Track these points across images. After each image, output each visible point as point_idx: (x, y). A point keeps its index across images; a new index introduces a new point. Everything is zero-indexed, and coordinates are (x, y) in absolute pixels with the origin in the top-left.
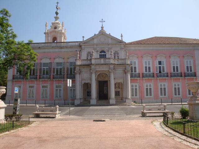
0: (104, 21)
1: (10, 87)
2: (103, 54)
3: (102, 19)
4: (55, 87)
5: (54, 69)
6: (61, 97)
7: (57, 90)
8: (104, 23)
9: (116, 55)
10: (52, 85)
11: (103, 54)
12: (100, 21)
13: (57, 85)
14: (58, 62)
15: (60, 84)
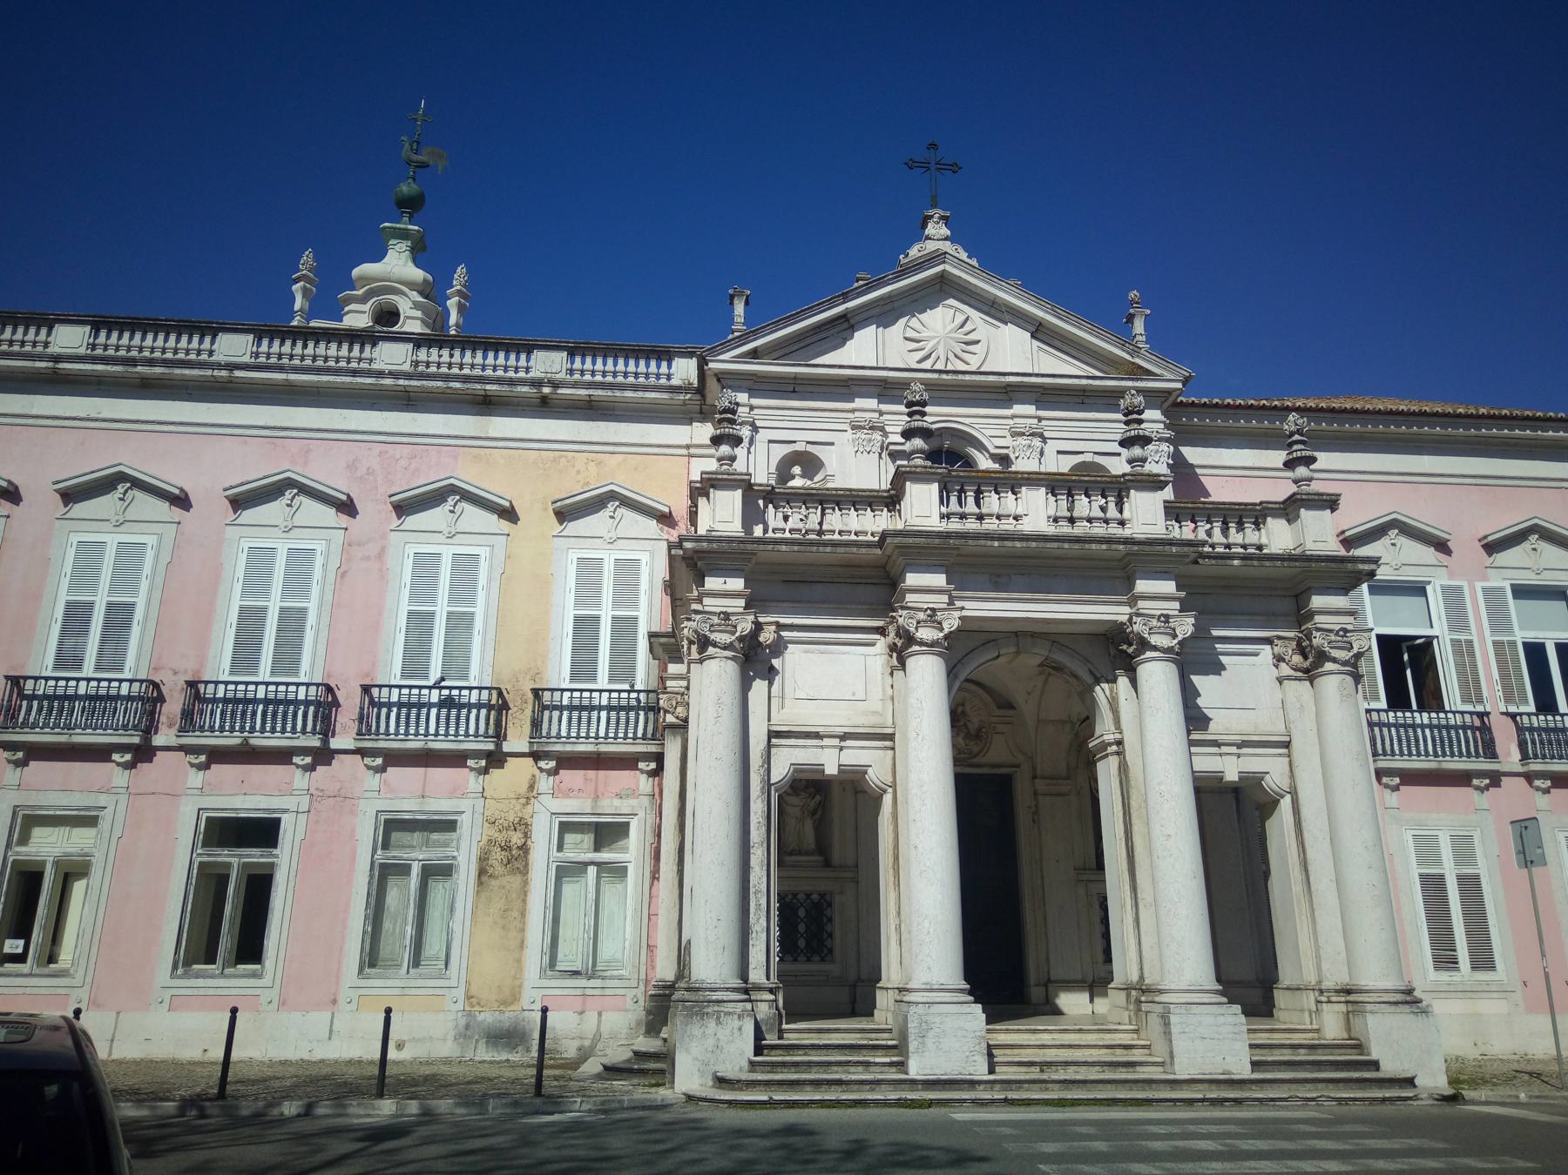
15: (439, 805)
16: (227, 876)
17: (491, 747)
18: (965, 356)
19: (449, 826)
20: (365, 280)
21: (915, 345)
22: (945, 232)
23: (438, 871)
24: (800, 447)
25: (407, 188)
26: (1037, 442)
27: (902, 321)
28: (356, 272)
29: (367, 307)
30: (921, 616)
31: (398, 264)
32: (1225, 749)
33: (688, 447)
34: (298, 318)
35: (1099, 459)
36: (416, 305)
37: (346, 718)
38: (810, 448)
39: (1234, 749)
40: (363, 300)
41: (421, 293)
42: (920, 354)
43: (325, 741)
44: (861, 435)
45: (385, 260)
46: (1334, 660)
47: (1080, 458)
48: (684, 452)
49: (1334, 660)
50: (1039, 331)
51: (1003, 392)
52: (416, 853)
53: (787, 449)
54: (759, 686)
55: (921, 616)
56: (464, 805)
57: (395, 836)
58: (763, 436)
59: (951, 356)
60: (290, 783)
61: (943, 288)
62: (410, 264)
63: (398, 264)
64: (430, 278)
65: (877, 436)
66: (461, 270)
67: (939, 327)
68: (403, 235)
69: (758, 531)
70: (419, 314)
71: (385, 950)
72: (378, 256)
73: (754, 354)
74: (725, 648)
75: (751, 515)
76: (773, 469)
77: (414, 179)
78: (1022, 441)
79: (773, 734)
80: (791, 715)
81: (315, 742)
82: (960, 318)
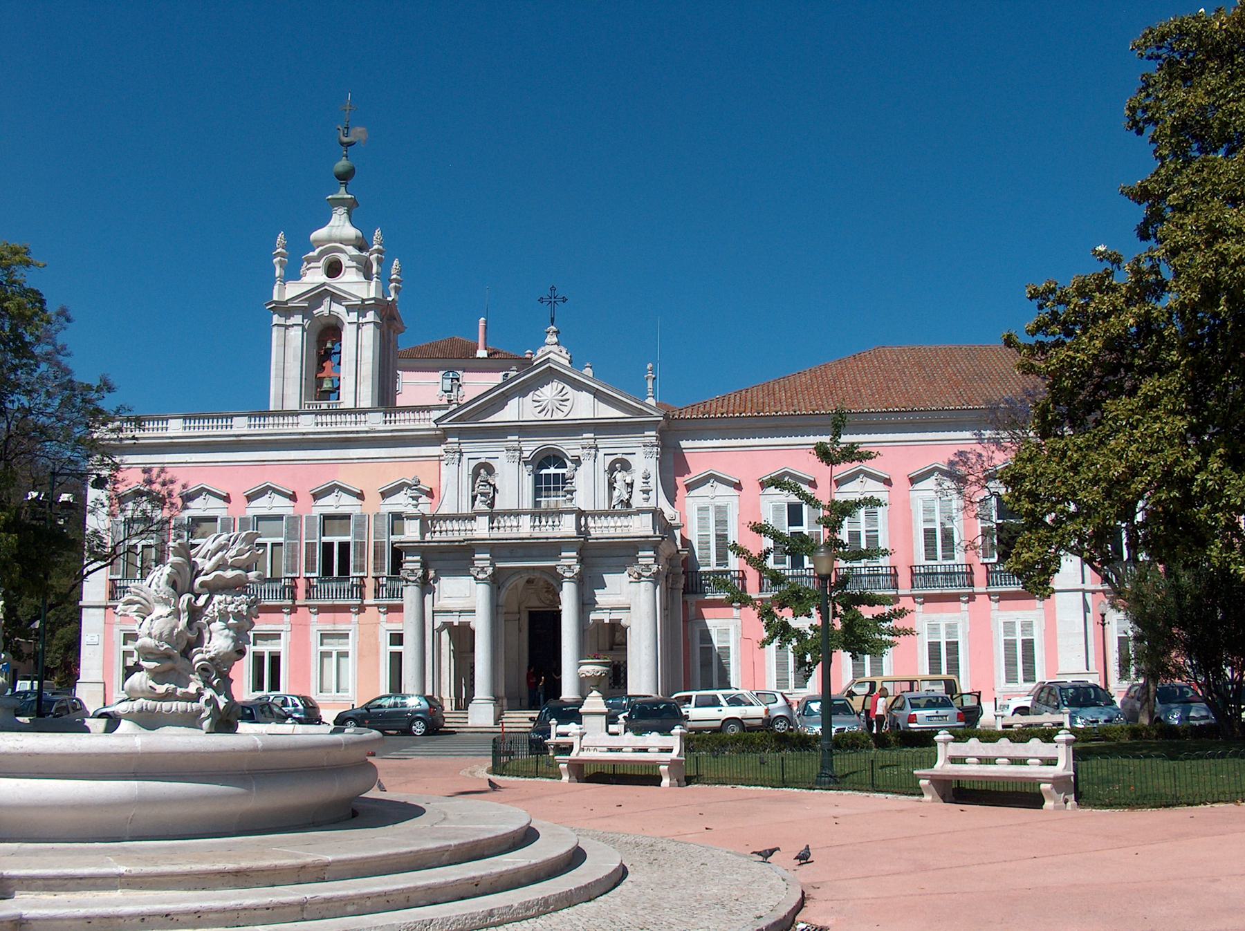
0: (564, 299)
1: (96, 639)
2: (552, 470)
3: (553, 289)
4: (314, 638)
5: (310, 547)
6: (347, 690)
7: (325, 655)
8: (560, 308)
9: (619, 476)
10: (300, 631)
11: (552, 470)
12: (541, 300)
13: (329, 627)
14: (331, 510)
15: (341, 627)
16: (263, 657)
17: (359, 602)
18: (560, 407)
19: (346, 636)
20: (320, 242)
21: (538, 404)
22: (555, 339)
23: (343, 655)
24: (483, 460)
25: (342, 165)
26: (593, 451)
27: (531, 394)
28: (315, 235)
29: (321, 264)
30: (479, 569)
31: (340, 226)
32: (605, 611)
33: (439, 456)
34: (278, 282)
35: (624, 457)
36: (352, 258)
37: (301, 592)
38: (488, 461)
39: (608, 611)
40: (317, 259)
41: (354, 246)
42: (540, 409)
43: (294, 603)
44: (510, 454)
45: (331, 223)
46: (644, 576)
47: (615, 457)
48: (437, 458)
49: (644, 576)
50: (597, 394)
51: (574, 429)
52: (333, 646)
53: (476, 462)
54: (428, 598)
55: (479, 569)
56: (349, 627)
57: (325, 641)
58: (466, 456)
59: (555, 409)
60: (283, 619)
61: (551, 374)
62: (348, 224)
63: (340, 226)
64: (360, 233)
65: (517, 454)
66: (378, 233)
67: (548, 394)
68: (340, 202)
69: (428, 537)
70: (354, 264)
71: (342, 686)
72: (325, 221)
73: (460, 419)
74: (413, 582)
75: (424, 530)
76: (470, 473)
77: (347, 157)
78: (585, 451)
79: (434, 612)
80: (442, 603)
81: (289, 602)
82: (560, 387)
